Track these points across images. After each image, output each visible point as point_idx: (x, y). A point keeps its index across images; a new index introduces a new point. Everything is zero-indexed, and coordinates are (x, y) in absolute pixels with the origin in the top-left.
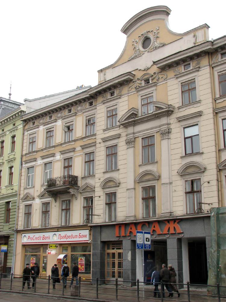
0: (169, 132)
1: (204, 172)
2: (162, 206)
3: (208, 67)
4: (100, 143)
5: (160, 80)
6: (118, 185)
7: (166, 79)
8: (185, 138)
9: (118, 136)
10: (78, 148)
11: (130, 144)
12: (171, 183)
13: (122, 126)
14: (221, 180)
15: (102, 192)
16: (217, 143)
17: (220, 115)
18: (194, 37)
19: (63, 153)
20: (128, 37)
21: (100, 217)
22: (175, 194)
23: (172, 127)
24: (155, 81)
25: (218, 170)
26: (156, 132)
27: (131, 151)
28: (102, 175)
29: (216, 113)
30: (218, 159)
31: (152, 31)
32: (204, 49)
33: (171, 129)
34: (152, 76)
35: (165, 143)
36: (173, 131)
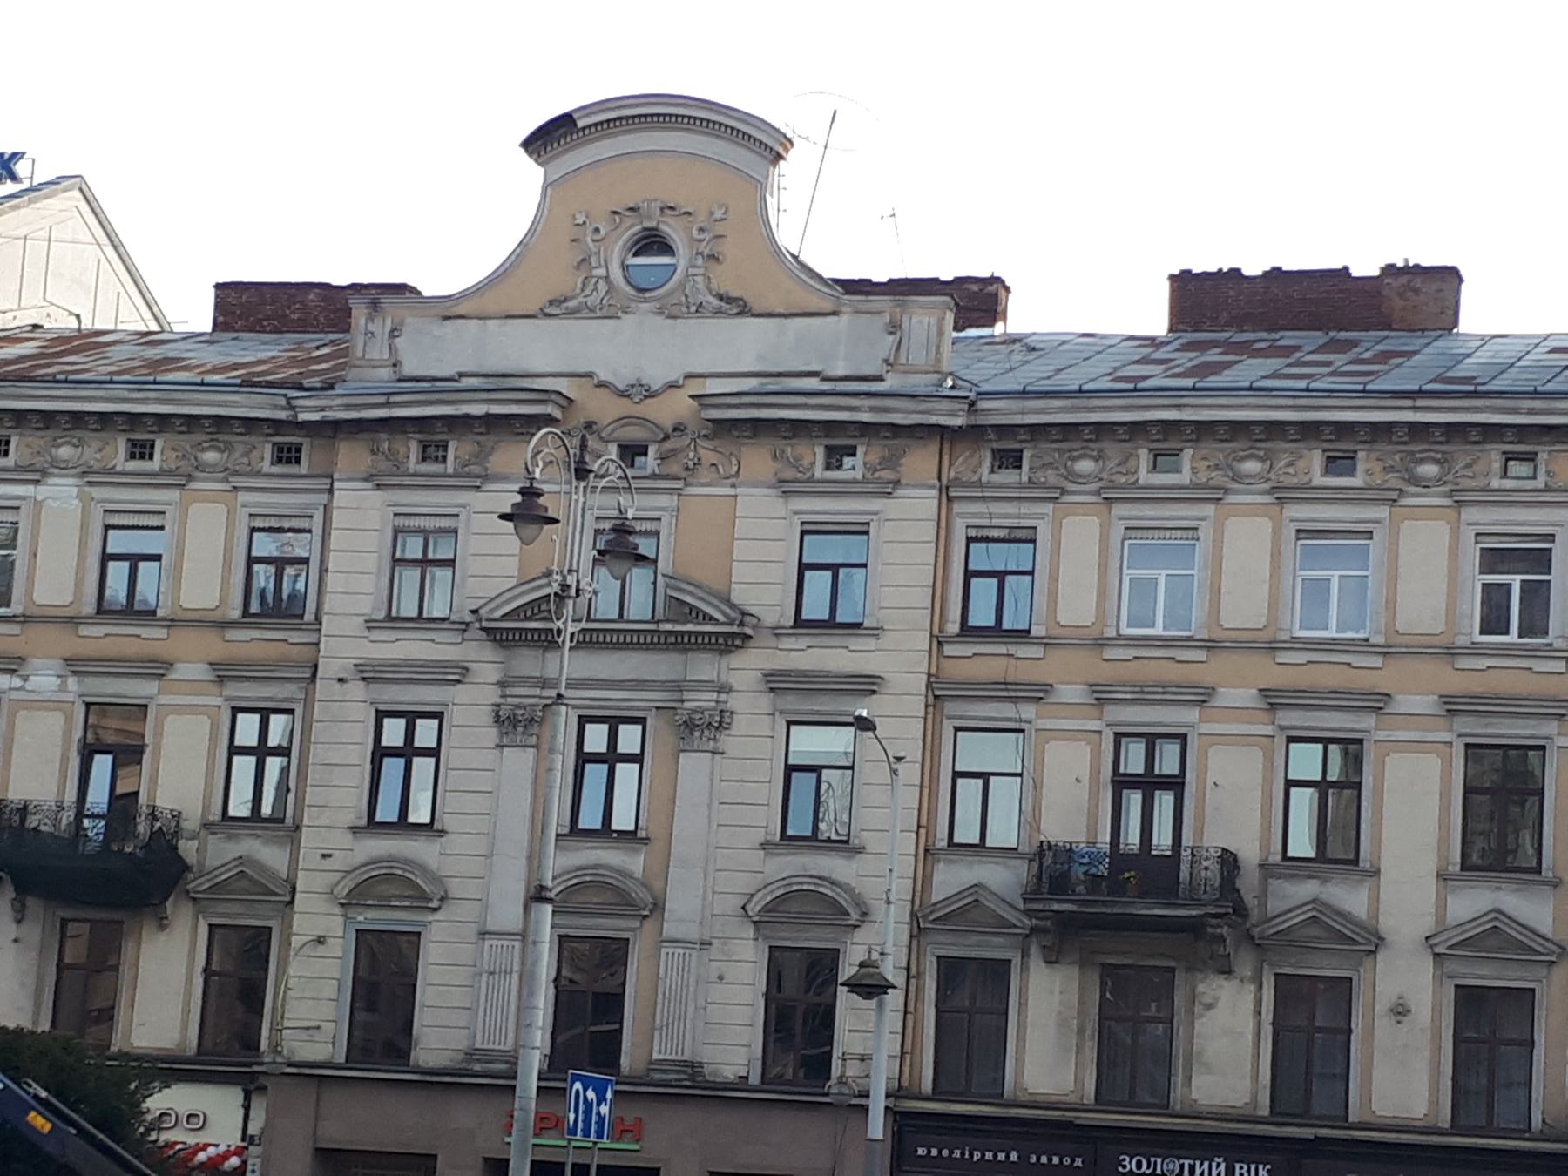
0: (721, 722)
1: (856, 927)
2: (657, 1034)
3: (935, 493)
4: (340, 680)
5: (704, 474)
6: (435, 904)
7: (733, 479)
8: (790, 770)
9: (459, 674)
10: (192, 670)
11: (520, 729)
12: (705, 944)
13: (474, 632)
14: (922, 968)
15: (340, 920)
16: (924, 822)
17: (950, 708)
18: (891, 333)
19: (76, 665)
20: (546, 186)
21: (317, 1036)
22: (717, 992)
23: (733, 702)
24: (674, 468)
25: (915, 931)
26: (657, 708)
27: (520, 761)
28: (346, 839)
29: (936, 697)
30: (919, 888)
31: (689, 213)
32: (933, 420)
33: (732, 713)
34: (666, 438)
35: (693, 765)
36: (740, 725)
